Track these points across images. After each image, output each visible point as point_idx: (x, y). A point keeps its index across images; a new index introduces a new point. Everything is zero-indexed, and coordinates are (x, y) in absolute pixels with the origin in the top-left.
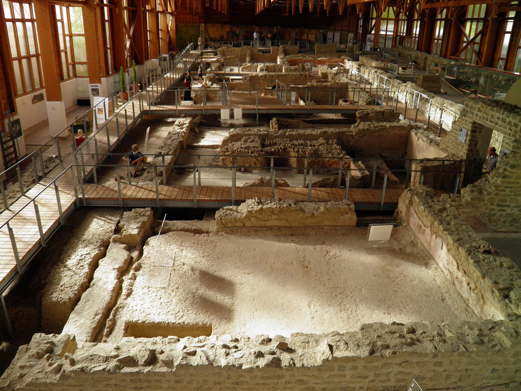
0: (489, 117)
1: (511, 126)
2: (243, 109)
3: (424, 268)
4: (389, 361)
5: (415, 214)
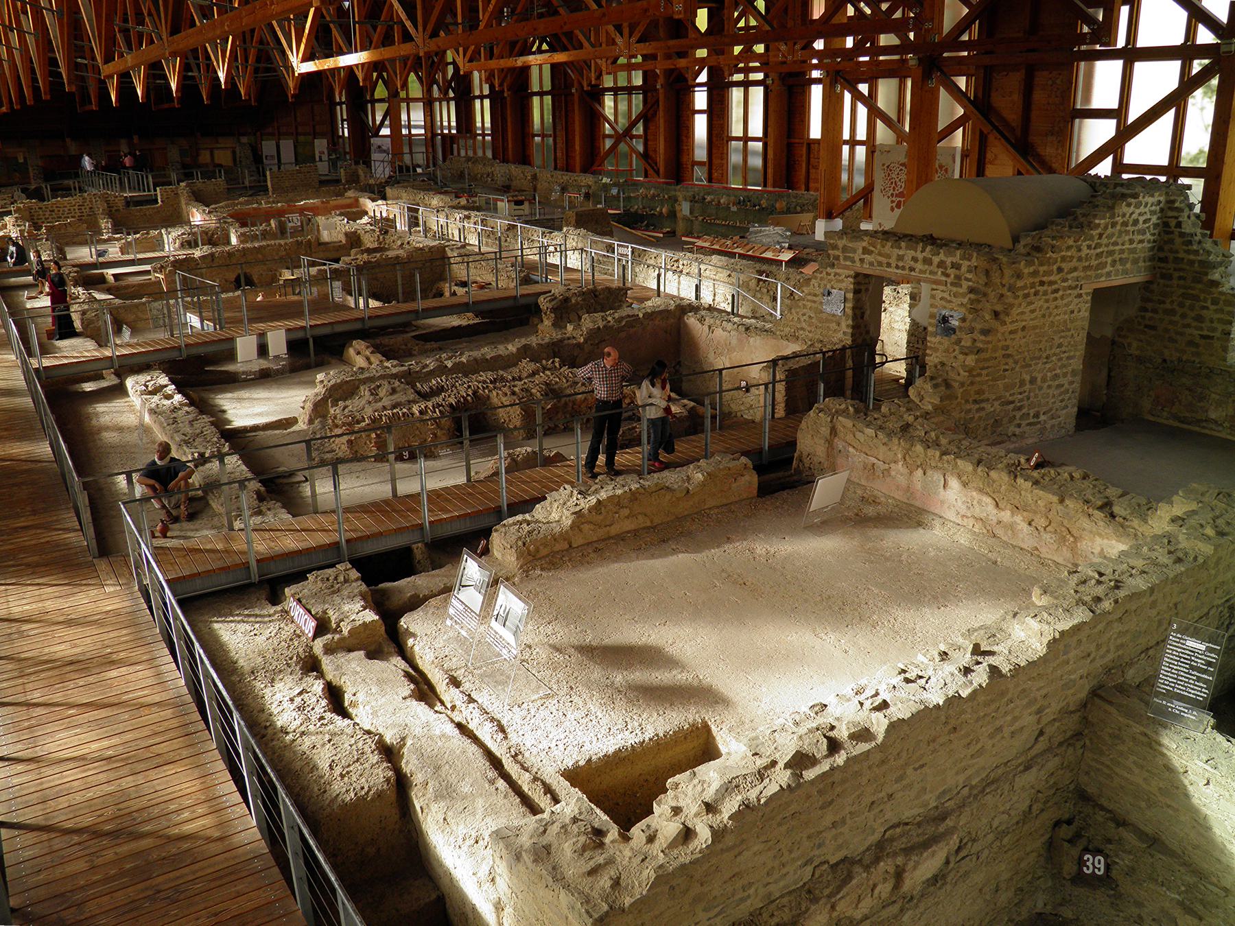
0: (893, 262)
2: (288, 330)
3: (921, 531)
4: (1110, 617)
5: (851, 449)
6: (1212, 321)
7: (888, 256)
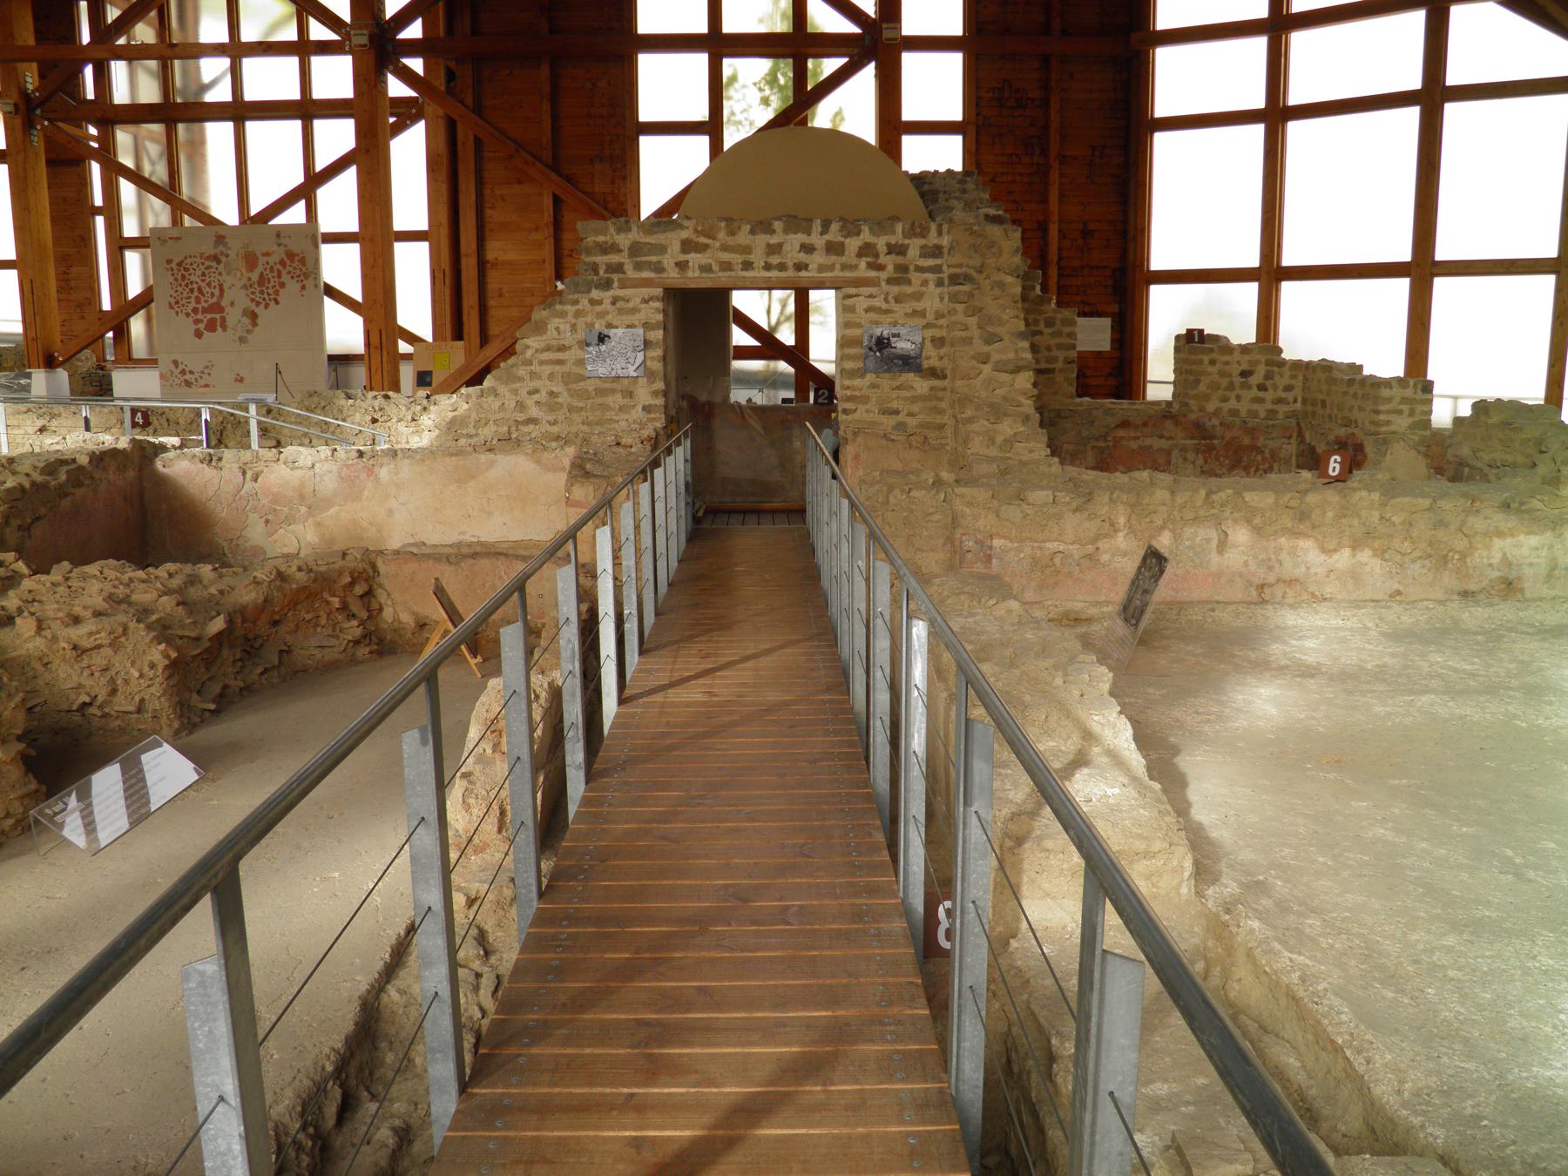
0: (758, 257)
1: (877, 256)
6: (1049, 349)
7: (747, 250)
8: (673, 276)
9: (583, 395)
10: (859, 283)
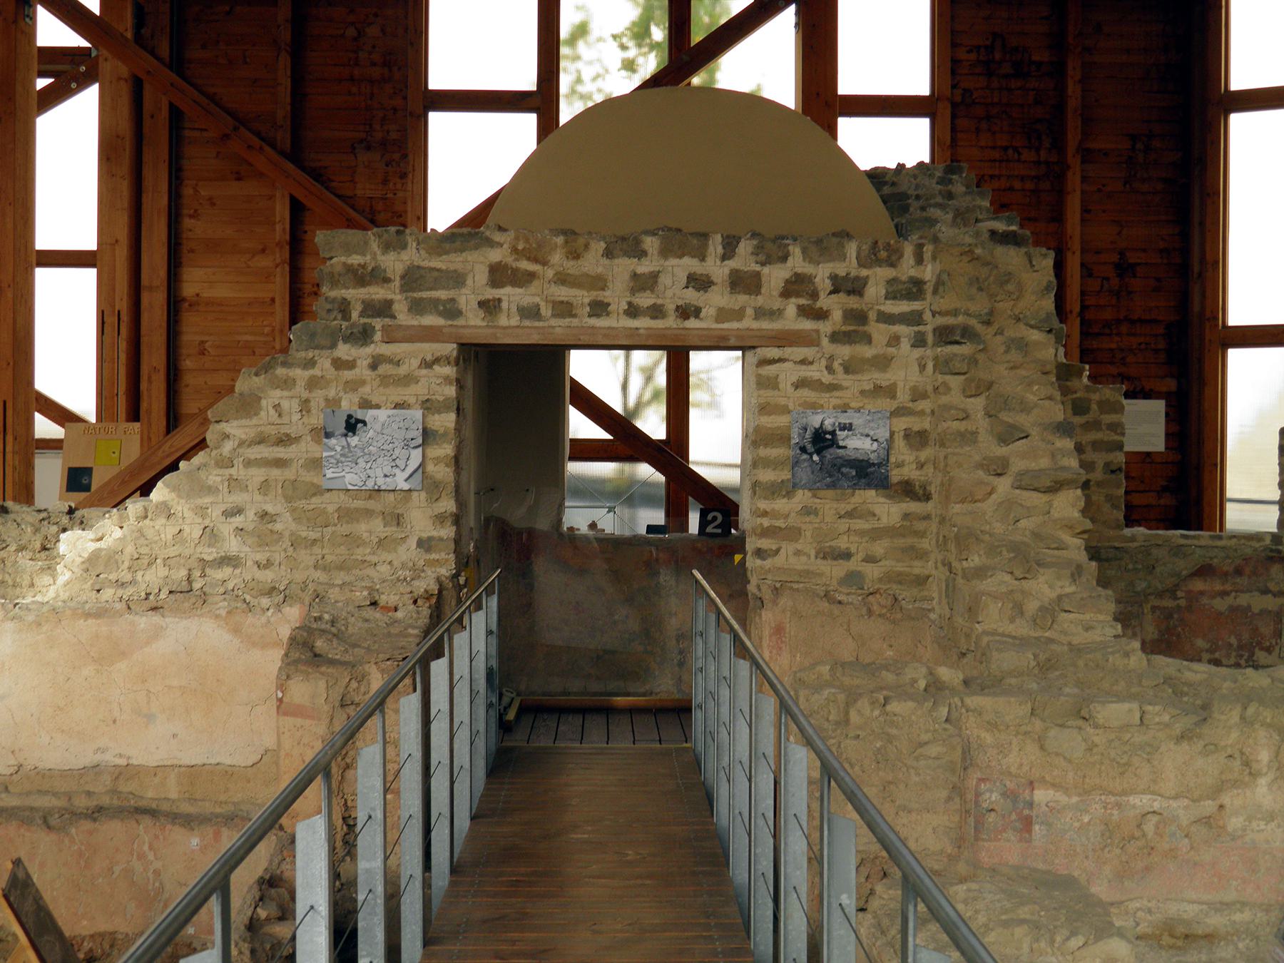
0: (617, 296)
1: (814, 295)
7: (599, 282)
8: (474, 325)
9: (317, 519)
10: (785, 339)
